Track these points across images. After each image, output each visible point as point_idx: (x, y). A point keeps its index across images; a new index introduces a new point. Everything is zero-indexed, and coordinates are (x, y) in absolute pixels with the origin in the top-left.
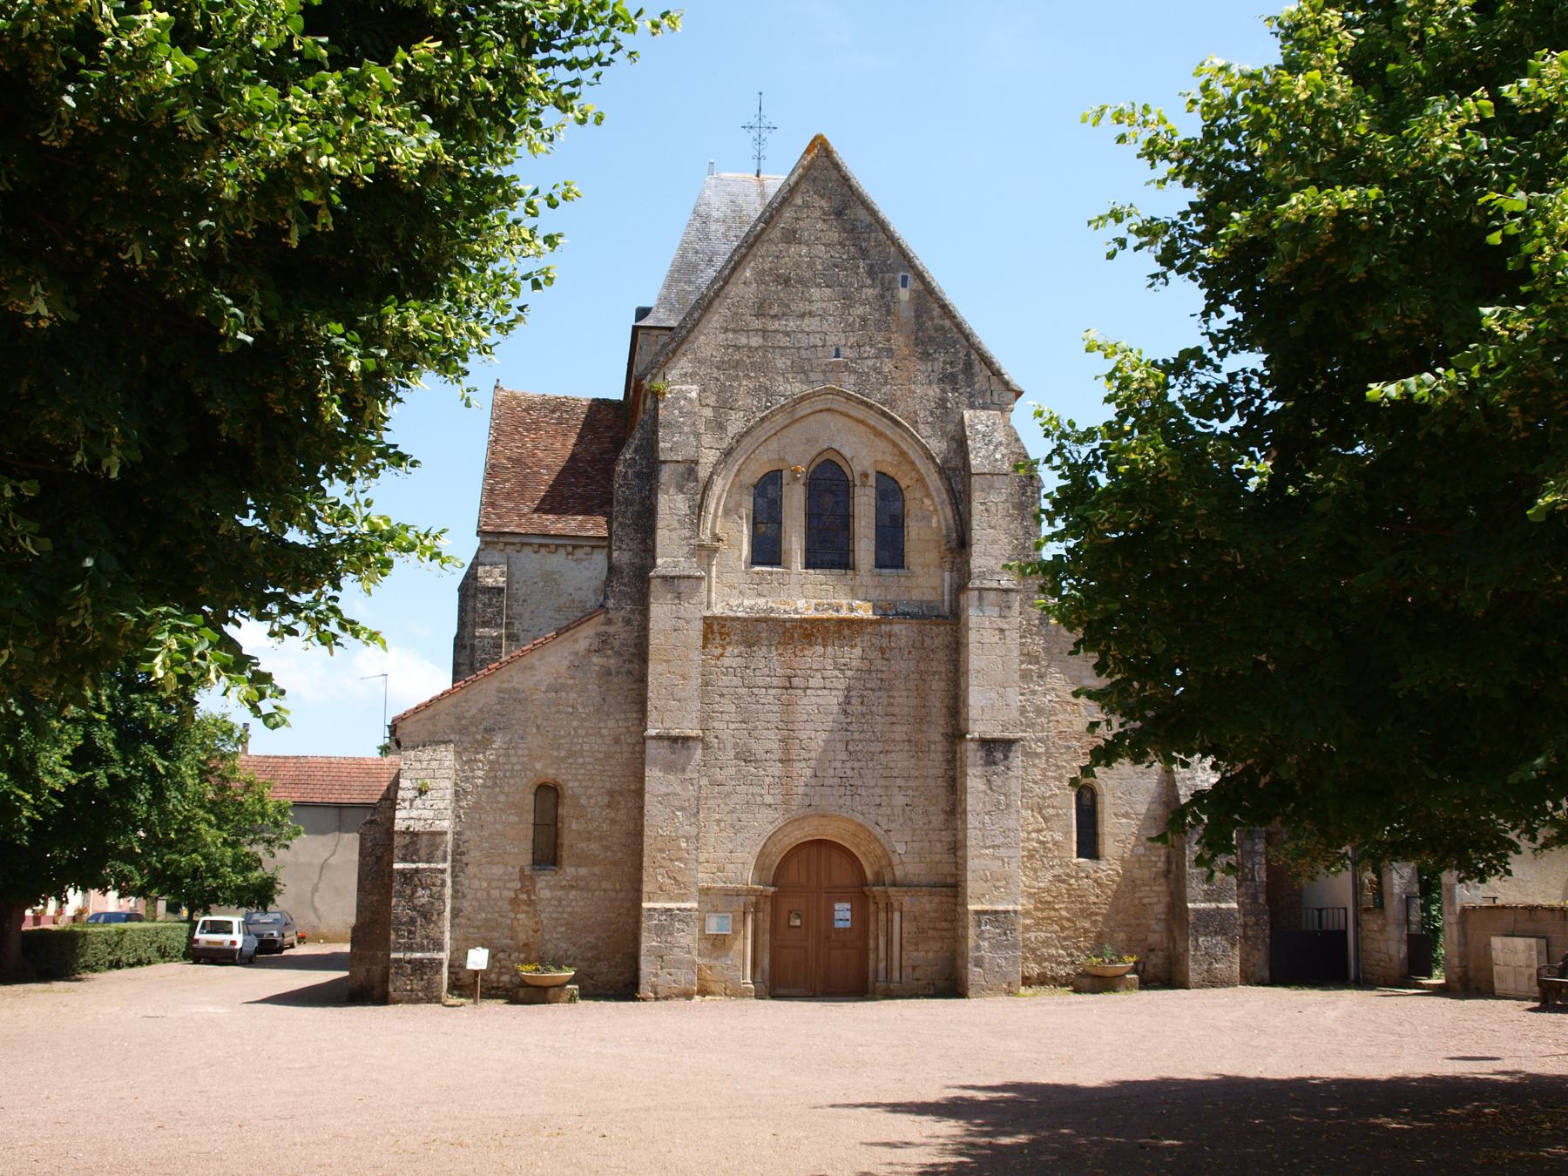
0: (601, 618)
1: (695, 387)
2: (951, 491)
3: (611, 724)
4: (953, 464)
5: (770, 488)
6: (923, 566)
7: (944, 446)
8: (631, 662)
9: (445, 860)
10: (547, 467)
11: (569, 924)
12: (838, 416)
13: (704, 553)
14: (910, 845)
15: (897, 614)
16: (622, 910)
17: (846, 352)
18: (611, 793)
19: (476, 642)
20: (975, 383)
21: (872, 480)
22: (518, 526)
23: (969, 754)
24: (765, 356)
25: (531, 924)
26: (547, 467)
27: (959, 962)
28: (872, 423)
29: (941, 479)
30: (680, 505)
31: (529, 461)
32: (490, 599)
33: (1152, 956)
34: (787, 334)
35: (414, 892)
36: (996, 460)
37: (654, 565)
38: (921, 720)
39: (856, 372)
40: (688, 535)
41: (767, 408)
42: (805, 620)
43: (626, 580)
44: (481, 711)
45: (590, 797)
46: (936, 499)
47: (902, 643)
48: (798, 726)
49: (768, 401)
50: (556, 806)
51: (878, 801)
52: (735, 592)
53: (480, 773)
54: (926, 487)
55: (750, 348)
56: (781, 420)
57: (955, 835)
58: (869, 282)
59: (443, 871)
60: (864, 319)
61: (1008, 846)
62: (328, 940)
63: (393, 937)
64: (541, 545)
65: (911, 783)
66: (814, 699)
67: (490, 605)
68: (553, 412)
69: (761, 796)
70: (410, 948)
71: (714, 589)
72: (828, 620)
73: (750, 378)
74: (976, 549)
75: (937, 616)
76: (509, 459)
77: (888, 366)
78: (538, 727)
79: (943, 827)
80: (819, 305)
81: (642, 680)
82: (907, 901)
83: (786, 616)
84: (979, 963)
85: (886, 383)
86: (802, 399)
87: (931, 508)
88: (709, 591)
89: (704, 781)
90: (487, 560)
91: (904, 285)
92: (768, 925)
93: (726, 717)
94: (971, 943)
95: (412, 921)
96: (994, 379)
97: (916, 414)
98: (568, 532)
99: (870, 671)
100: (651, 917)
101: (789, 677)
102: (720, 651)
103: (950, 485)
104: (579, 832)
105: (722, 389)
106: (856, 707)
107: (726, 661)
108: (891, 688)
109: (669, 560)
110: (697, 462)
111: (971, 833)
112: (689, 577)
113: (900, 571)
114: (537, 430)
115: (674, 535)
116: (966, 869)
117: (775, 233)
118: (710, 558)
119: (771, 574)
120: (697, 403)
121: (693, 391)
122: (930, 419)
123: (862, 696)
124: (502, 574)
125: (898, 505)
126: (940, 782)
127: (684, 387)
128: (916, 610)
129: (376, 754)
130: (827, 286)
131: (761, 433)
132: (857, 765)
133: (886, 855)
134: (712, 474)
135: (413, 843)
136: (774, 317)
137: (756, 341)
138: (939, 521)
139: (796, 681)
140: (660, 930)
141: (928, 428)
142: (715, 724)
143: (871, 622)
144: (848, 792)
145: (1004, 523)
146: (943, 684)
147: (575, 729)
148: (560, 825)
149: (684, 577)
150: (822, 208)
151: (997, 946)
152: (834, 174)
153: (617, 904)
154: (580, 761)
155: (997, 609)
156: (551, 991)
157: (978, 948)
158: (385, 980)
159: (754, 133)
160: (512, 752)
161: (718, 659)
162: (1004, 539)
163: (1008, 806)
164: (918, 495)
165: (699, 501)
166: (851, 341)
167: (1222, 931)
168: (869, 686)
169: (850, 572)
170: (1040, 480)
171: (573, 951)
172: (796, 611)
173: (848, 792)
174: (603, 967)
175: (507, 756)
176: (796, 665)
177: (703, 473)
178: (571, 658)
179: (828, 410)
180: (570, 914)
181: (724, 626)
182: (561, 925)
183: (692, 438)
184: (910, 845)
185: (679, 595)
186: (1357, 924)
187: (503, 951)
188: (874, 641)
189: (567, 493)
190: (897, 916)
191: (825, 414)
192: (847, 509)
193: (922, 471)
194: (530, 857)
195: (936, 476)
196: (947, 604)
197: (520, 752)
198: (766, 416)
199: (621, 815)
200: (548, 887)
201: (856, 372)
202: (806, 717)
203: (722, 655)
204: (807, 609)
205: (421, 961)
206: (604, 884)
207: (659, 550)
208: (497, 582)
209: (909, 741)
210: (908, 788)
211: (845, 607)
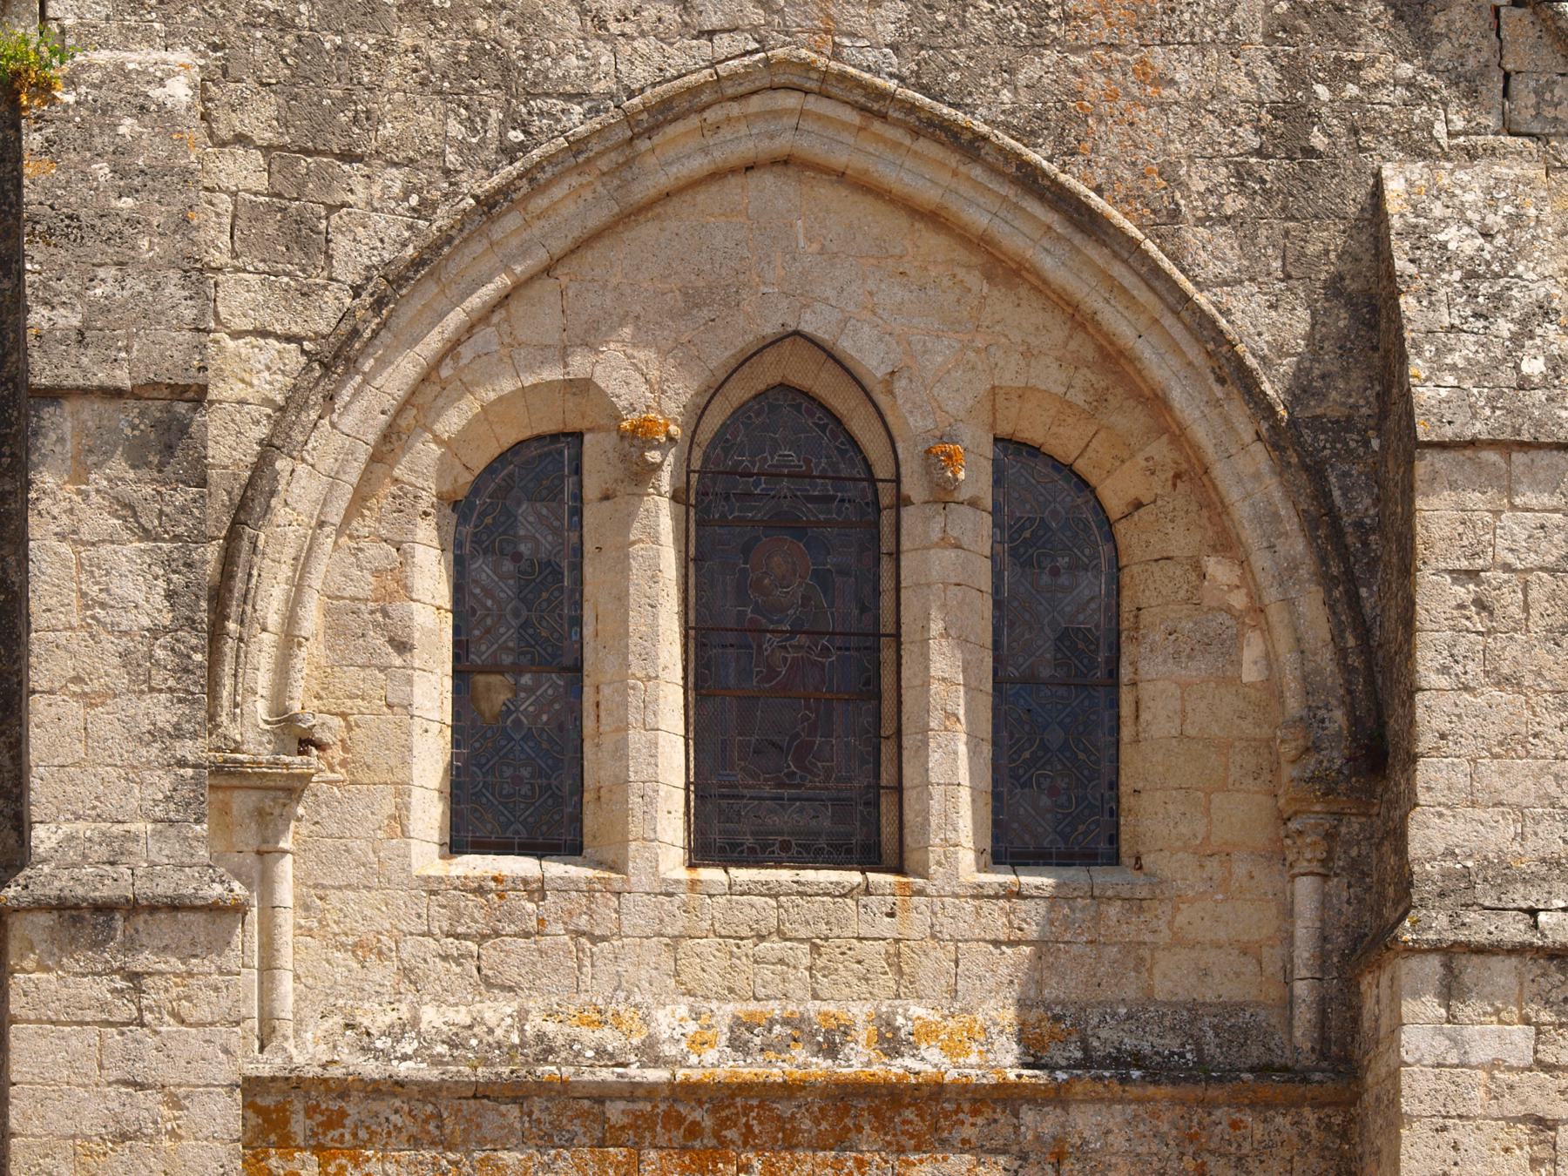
1: (181, 56)
4: (1333, 405)
5: (527, 517)
6: (1204, 853)
7: (1299, 321)
12: (827, 193)
13: (242, 802)
15: (1087, 1062)
28: (978, 219)
29: (1282, 467)
30: (127, 587)
36: (1524, 384)
40: (165, 719)
41: (510, 152)
42: (690, 1091)
46: (1261, 560)
52: (382, 974)
54: (1212, 505)
71: (286, 957)
72: (789, 1089)
75: (1263, 1070)
83: (606, 1075)
85: (1037, 43)
86: (666, 112)
87: (1238, 600)
88: (268, 967)
97: (1175, 182)
103: (1322, 494)
109: (83, 828)
110: (198, 396)
112: (175, 906)
113: (1103, 877)
115: (105, 721)
118: (269, 822)
119: (537, 890)
120: (197, 131)
122: (1233, 204)
125: (1091, 586)
127: (134, 59)
128: (1171, 1043)
134: (269, 448)
138: (1270, 659)
141: (1224, 240)
149: (153, 909)
164: (1181, 541)
165: (211, 569)
172: (650, 1053)
179: (784, 162)
183: (173, 289)
191: (767, 181)
192: (868, 602)
193: (1201, 433)
195: (1260, 456)
196: (1304, 1016)
198: (504, 191)
204: (699, 1043)
207: (42, 789)
211: (862, 1033)
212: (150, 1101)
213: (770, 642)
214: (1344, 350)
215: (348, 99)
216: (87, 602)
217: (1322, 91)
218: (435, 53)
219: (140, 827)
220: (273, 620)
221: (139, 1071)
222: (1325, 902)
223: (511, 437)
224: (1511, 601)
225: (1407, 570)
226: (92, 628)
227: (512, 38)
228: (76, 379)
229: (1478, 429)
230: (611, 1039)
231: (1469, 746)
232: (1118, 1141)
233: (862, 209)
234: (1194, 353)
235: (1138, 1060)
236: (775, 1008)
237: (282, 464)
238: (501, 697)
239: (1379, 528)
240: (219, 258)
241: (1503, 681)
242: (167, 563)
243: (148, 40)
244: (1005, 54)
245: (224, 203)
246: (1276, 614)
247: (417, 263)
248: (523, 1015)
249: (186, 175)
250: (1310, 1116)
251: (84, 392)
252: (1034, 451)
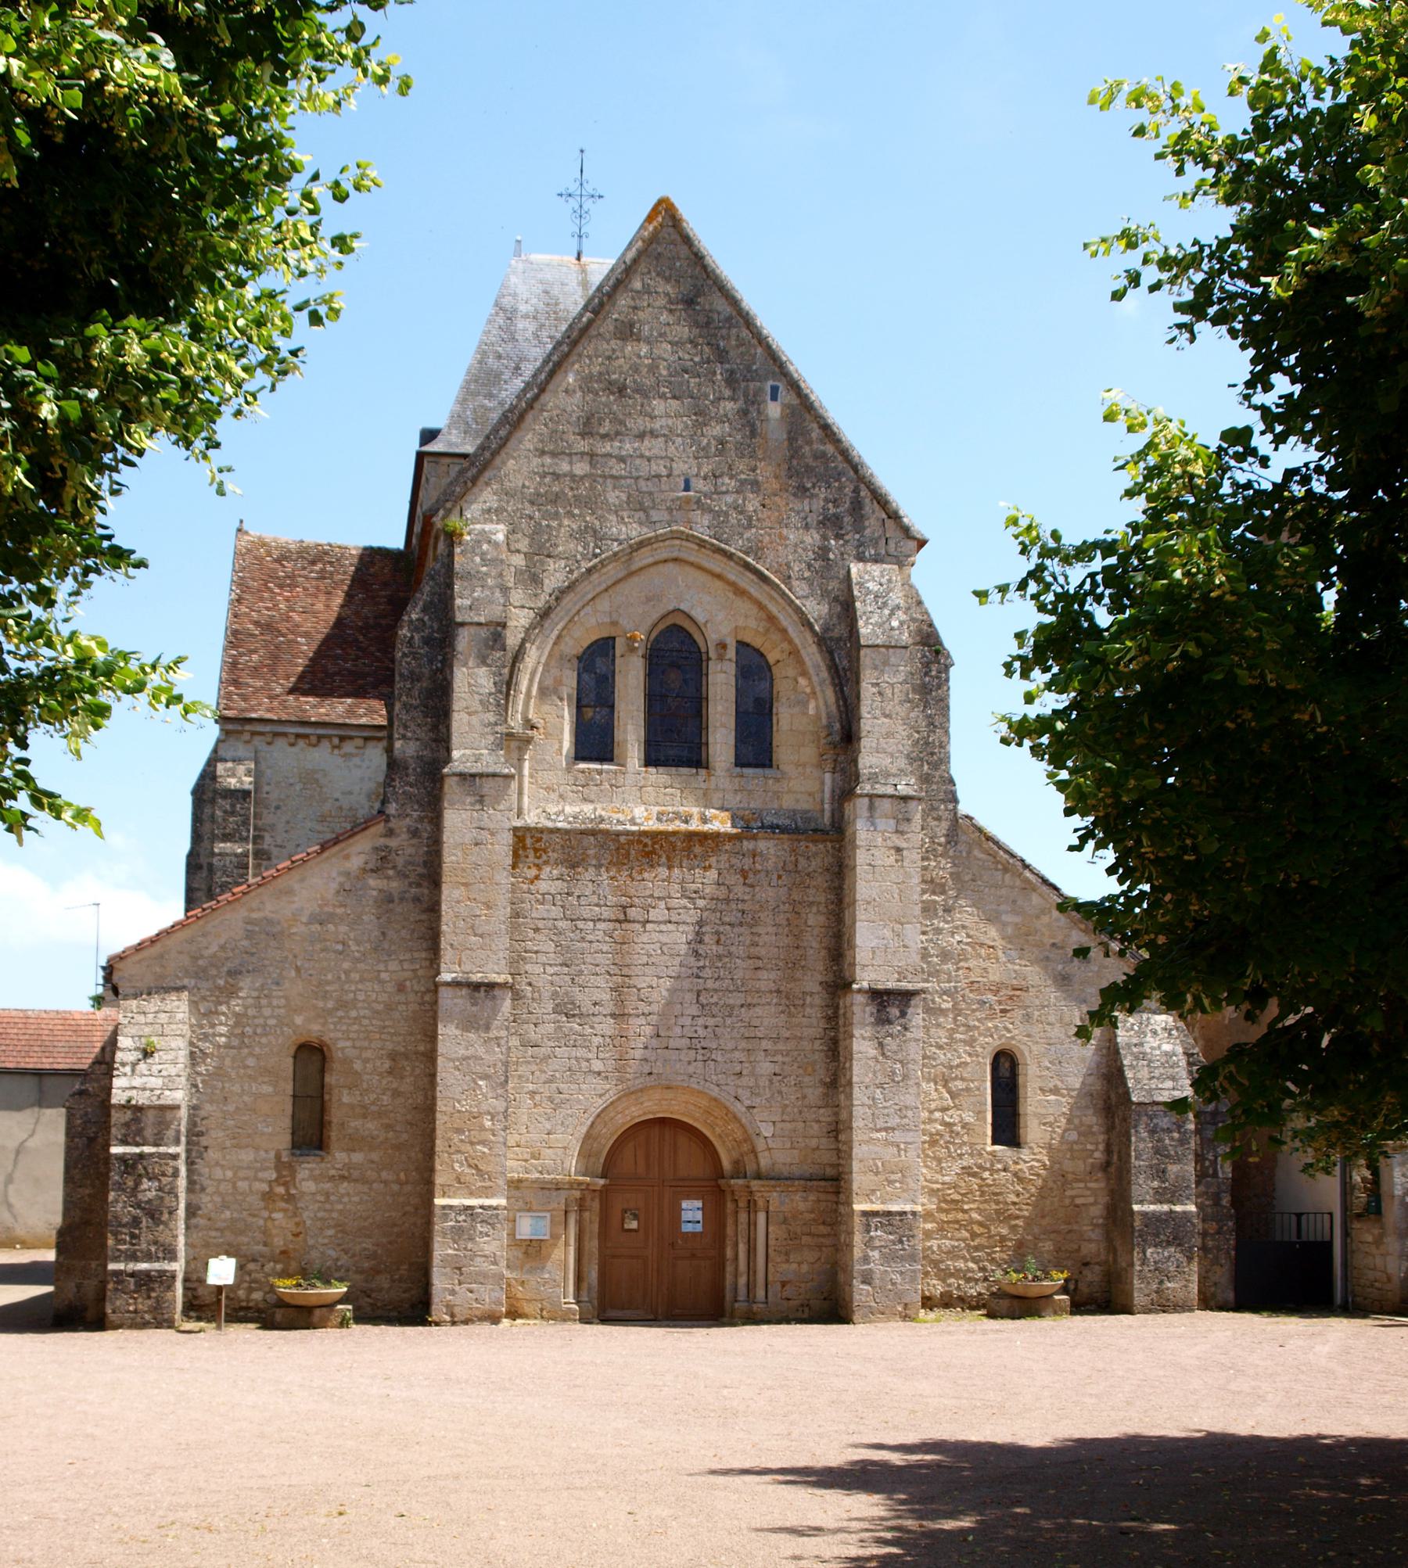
0: (380, 828)
1: (501, 527)
2: (833, 668)
3: (393, 966)
4: (836, 633)
5: (599, 662)
6: (797, 765)
7: (824, 609)
8: (419, 885)
9: (177, 1142)
10: (306, 635)
11: (341, 1227)
12: (687, 568)
13: (514, 744)
14: (779, 1125)
15: (762, 827)
16: (408, 1208)
17: (699, 484)
18: (393, 1056)
19: (215, 860)
20: (865, 528)
21: (731, 653)
22: (268, 710)
23: (856, 1009)
24: (592, 488)
26: (306, 635)
27: (841, 1277)
28: (732, 577)
29: (821, 651)
30: (483, 681)
31: (283, 627)
32: (233, 806)
33: (1086, 1272)
34: (622, 459)
35: (137, 1184)
36: (892, 629)
37: (448, 759)
38: (793, 965)
39: (711, 511)
40: (492, 719)
41: (596, 556)
42: (645, 833)
43: (412, 779)
44: (223, 948)
45: (366, 1061)
46: (815, 679)
47: (770, 865)
48: (637, 970)
49: (596, 546)
50: (322, 1071)
51: (738, 1069)
52: (554, 796)
53: (223, 1029)
54: (800, 662)
55: (573, 477)
56: (613, 571)
57: (836, 1114)
58: (727, 393)
59: (175, 1157)
60: (722, 442)
61: (905, 1128)
62: (26, 1245)
63: (110, 1242)
64: (298, 736)
65: (781, 1046)
66: (655, 936)
67: (233, 813)
68: (313, 563)
69: (588, 1060)
70: (133, 1257)
71: (526, 791)
72: (674, 833)
73: (574, 516)
74: (867, 744)
75: (815, 831)
76: (257, 623)
77: (752, 504)
78: (298, 969)
79: (820, 1103)
80: (663, 422)
81: (433, 909)
82: (776, 1199)
83: (620, 828)
84: (867, 1279)
85: (750, 526)
86: (641, 545)
88: (520, 793)
89: (514, 1041)
90: (229, 755)
91: (774, 398)
92: (596, 1227)
93: (542, 958)
94: (857, 1253)
95: (136, 1222)
96: (889, 523)
97: (789, 567)
98: (333, 718)
99: (727, 901)
100: (445, 1217)
101: (624, 907)
102: (534, 872)
103: (833, 659)
104: (352, 1107)
105: (538, 530)
106: (710, 947)
107: (543, 886)
108: (756, 922)
109: (468, 752)
110: (504, 626)
111: (858, 1111)
112: (494, 775)
113: (767, 771)
114: (293, 586)
115: (475, 720)
116: (850, 1156)
117: (607, 327)
118: (521, 750)
119: (600, 772)
120: (505, 548)
121: (499, 532)
122: (807, 574)
123: (717, 933)
124: (248, 773)
125: (765, 685)
126: (817, 1045)
127: (487, 527)
128: (787, 822)
129: (86, 1006)
130: (674, 397)
131: (588, 589)
132: (711, 1022)
133: (747, 1139)
134: (524, 641)
135: (136, 1120)
136: (604, 436)
137: (581, 468)
138: (817, 707)
139: (633, 913)
140: (458, 1233)
142: (528, 967)
143: (730, 837)
144: (700, 1057)
145: (902, 710)
146: (822, 919)
147: (347, 973)
148: (327, 1097)
149: (488, 775)
150: (667, 294)
151: (889, 1258)
152: (684, 250)
153: (401, 1199)
154: (354, 1014)
155: (892, 822)
156: (317, 1312)
157: (866, 1259)
158: (101, 1298)
159: (574, 203)
160: (264, 1002)
161: (532, 882)
162: (902, 731)
163: (905, 1077)
164: (791, 672)
165: (506, 677)
166: (705, 470)
167: (1176, 1240)
168: (727, 919)
169: (702, 772)
170: (948, 656)
171: (344, 1260)
172: (633, 822)
173: (700, 1057)
174: (383, 1281)
175: (259, 1007)
176: (632, 892)
177: (512, 639)
178: (342, 879)
179: (675, 560)
180: (340, 1212)
181: (539, 840)
182: (328, 1228)
183: (498, 594)
184: (779, 1125)
185: (481, 800)
186: (1346, 1234)
187: (254, 1260)
188: (734, 861)
189: (332, 669)
190: (761, 1218)
191: (671, 565)
192: (699, 689)
193: (797, 641)
194: (288, 1138)
195: (814, 649)
196: (827, 815)
197: (275, 1002)
198: (594, 567)
199: (406, 1085)
200: (315, 1179)
201: (711, 511)
202: (645, 959)
203: (537, 877)
204: (647, 819)
205: (147, 1273)
206: (384, 1175)
207: (455, 739)
208: (241, 782)
209: (778, 991)
210: (776, 1052)
211: (696, 817)
212: (485, 833)
213: (670, 700)
214: (839, 617)
215: (549, 540)
216: (470, 685)
217: (833, 542)
218: (575, 527)
219: (485, 752)
220: (524, 690)
221: (482, 824)
222: (833, 780)
223: (594, 638)
224: (889, 692)
225: (858, 682)
226: (472, 693)
227: (597, 523)
228: (469, 620)
229: (879, 642)
230: (622, 817)
231: (877, 735)
232: (772, 851)
233: (698, 574)
234: (795, 617)
235: (778, 827)
236: (670, 809)
237: (528, 645)
238: (590, 714)
239: (850, 669)
240: (511, 585)
241: (886, 716)
242: (494, 674)
243: (492, 521)
244: (741, 530)
245: (513, 569)
246: (819, 694)
247: (568, 587)
248: (595, 809)
249: (502, 561)
250: (829, 845)
251: (471, 624)
252: (748, 645)
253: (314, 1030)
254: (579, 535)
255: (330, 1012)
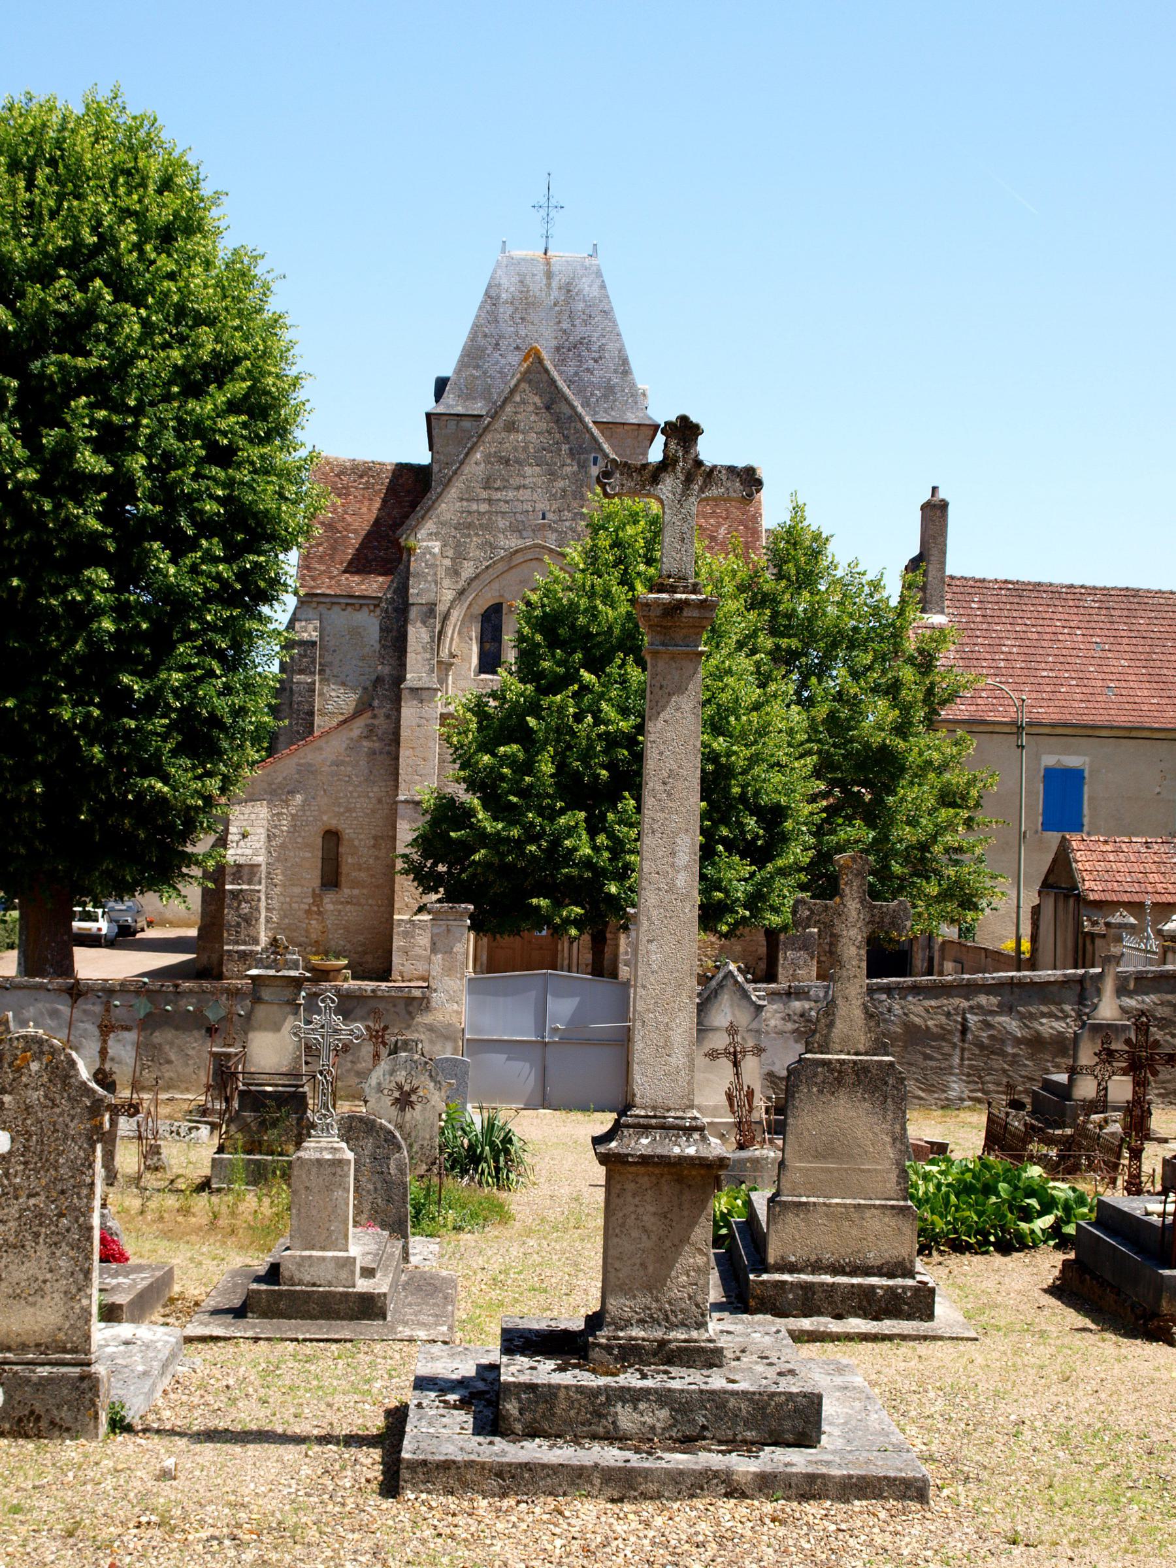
0: (369, 714)
1: (438, 543)
3: (376, 789)
8: (390, 745)
9: (260, 883)
11: (346, 929)
13: (443, 666)
17: (550, 516)
18: (375, 838)
24: (490, 519)
25: (320, 928)
34: (507, 502)
35: (239, 905)
39: (557, 531)
44: (285, 779)
45: (360, 840)
50: (338, 845)
53: (285, 822)
55: (479, 513)
56: (501, 567)
58: (569, 461)
59: (259, 891)
60: (564, 491)
63: (225, 935)
70: (237, 943)
80: (531, 480)
81: (397, 758)
86: (516, 552)
91: (595, 464)
95: (238, 925)
104: (353, 865)
105: (458, 544)
117: (499, 425)
118: (447, 670)
121: (436, 547)
127: (430, 544)
131: (486, 577)
135: (239, 872)
136: (497, 489)
137: (484, 507)
150: (535, 404)
152: (545, 377)
154: (354, 815)
156: (332, 974)
158: (221, 964)
166: (554, 507)
171: (348, 947)
174: (369, 958)
175: (304, 811)
177: (441, 608)
194: (319, 881)
199: (382, 854)
200: (333, 903)
201: (557, 531)
205: (244, 952)
206: (370, 901)
253: (333, 823)
254: (481, 547)
255: (342, 814)
